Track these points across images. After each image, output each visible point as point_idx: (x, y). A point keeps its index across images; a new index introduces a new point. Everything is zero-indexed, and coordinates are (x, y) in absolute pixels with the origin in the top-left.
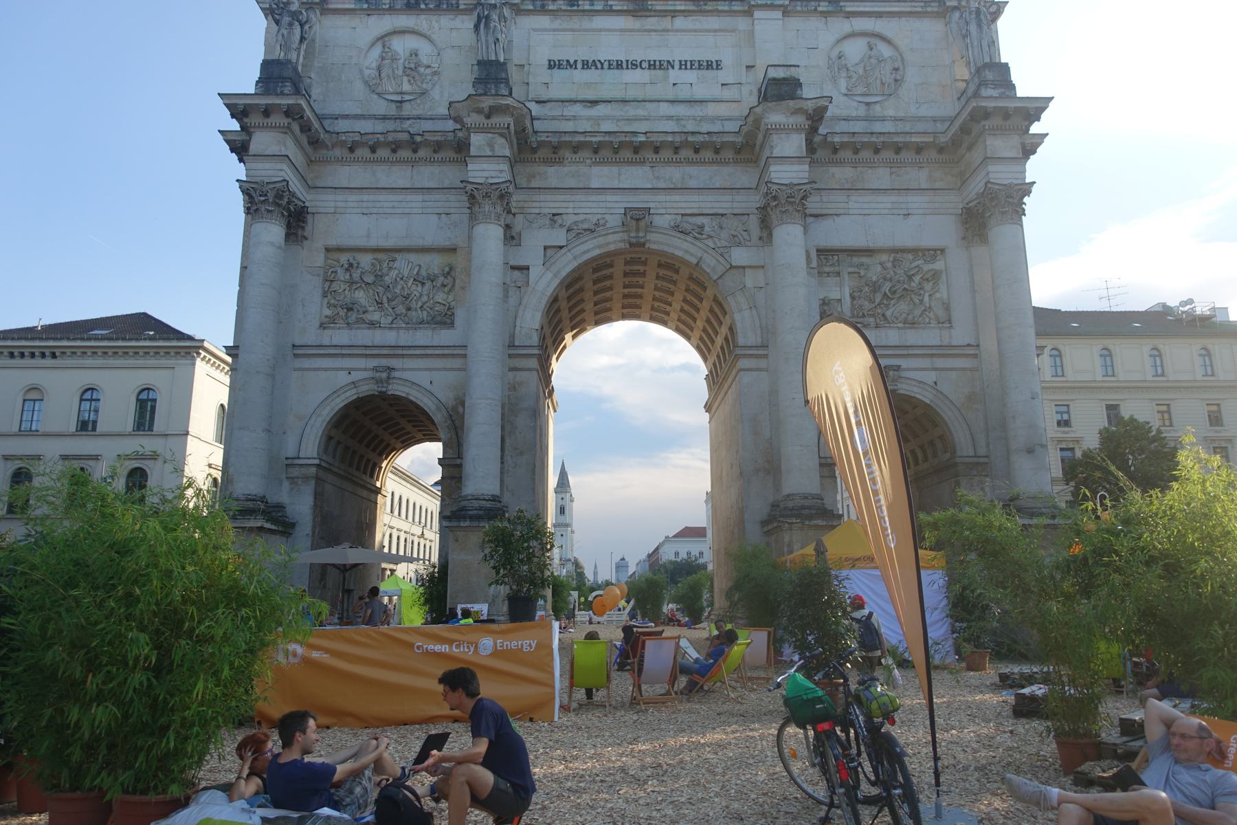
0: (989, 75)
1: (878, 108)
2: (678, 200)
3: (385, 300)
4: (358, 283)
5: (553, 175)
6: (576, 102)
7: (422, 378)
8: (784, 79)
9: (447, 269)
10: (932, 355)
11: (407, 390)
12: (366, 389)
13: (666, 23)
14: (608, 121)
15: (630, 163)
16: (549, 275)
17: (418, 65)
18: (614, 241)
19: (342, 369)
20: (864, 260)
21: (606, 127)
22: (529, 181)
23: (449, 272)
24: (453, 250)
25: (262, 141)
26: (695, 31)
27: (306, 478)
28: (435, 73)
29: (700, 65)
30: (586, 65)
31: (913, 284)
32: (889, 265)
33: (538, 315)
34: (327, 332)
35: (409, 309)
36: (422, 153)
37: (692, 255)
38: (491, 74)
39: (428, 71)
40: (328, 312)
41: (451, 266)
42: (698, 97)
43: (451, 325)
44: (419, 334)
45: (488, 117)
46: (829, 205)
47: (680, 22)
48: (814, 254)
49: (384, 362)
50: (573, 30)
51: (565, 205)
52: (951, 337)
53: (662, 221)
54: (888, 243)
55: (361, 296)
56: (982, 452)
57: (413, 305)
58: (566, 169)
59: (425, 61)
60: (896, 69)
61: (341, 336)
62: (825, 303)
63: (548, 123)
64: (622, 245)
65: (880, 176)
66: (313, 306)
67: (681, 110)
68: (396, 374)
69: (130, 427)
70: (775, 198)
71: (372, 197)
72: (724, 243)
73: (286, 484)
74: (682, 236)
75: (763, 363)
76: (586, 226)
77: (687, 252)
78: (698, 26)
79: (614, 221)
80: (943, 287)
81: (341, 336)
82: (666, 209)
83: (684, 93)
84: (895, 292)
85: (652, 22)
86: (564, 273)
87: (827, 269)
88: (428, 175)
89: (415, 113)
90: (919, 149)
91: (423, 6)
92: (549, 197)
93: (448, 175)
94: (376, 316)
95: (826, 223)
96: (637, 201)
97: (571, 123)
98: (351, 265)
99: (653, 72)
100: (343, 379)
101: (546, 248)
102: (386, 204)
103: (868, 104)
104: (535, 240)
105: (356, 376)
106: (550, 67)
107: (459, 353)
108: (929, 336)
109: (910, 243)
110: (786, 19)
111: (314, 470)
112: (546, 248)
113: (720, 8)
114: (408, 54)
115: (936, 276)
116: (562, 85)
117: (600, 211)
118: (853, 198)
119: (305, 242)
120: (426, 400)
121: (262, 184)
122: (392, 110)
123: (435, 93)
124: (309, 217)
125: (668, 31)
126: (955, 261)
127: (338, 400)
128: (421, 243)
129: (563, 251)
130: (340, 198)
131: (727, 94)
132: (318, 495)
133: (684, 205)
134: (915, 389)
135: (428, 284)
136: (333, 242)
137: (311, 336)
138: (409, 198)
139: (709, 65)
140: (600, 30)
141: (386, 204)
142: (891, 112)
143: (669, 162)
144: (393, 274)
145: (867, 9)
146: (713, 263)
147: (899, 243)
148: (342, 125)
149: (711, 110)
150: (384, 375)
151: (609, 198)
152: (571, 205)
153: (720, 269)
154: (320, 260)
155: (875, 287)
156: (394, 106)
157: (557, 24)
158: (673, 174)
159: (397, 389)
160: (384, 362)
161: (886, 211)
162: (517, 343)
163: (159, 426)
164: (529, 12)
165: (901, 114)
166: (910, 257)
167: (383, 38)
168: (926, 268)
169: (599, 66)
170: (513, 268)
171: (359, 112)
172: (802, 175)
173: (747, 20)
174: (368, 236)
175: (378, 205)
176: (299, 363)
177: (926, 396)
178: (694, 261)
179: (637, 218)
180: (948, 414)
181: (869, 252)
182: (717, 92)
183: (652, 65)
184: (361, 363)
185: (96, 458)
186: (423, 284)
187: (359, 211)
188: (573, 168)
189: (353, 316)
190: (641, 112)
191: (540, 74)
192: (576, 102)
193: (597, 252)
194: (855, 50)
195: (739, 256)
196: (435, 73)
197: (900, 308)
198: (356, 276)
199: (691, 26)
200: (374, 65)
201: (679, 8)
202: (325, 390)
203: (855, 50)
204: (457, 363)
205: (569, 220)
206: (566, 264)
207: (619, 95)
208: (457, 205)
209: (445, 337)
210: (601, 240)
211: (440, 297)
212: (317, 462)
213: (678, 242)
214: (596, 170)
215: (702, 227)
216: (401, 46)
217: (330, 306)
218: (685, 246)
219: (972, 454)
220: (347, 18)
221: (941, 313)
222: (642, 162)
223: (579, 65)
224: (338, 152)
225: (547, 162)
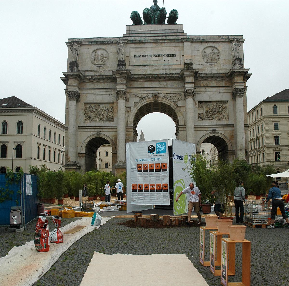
0: (237, 62)
1: (213, 66)
2: (166, 92)
3: (98, 115)
4: (91, 111)
5: (136, 84)
6: (141, 66)
7: (107, 134)
8: (189, 63)
9: (112, 107)
10: (223, 127)
11: (104, 136)
12: (95, 136)
13: (163, 45)
14: (148, 71)
15: (154, 81)
16: (135, 109)
17: (103, 57)
18: (150, 100)
19: (89, 132)
20: (209, 104)
21: (149, 72)
22: (130, 86)
23: (112, 108)
24: (113, 103)
25: (71, 82)
26: (170, 47)
27: (83, 156)
28: (107, 59)
29: (171, 56)
30: (143, 56)
31: (220, 110)
32: (215, 105)
33: (133, 119)
34: (86, 123)
35: (103, 117)
36: (105, 80)
37: (168, 103)
38: (121, 63)
39: (106, 58)
40: (85, 118)
41: (112, 106)
42: (170, 64)
43: (113, 121)
44: (106, 123)
45: (121, 75)
46: (201, 91)
47: (166, 45)
49: (99, 130)
50: (140, 47)
51: (139, 92)
52: (228, 122)
53: (161, 95)
54: (215, 100)
55: (92, 114)
56: (234, 149)
57: (104, 116)
58: (139, 83)
59: (105, 56)
60: (218, 56)
61: (89, 124)
62: (200, 114)
63: (134, 72)
64: (152, 101)
65: (213, 83)
66: (83, 118)
67: (166, 67)
68: (101, 133)
69: (16, 133)
70: (187, 92)
71: (94, 91)
72: (176, 101)
73: (79, 158)
74: (166, 99)
75: (184, 129)
76: (144, 97)
77: (167, 102)
78: (170, 46)
79: (150, 95)
80: (227, 110)
81: (89, 124)
82: (162, 93)
84: (216, 112)
85: (159, 45)
86: (139, 108)
87: (200, 106)
88: (107, 85)
90: (222, 77)
91: (104, 43)
92: (135, 90)
93: (111, 85)
95: (200, 95)
96: (156, 91)
97: (140, 71)
98: (90, 107)
99: (159, 57)
100: (90, 134)
101: (134, 102)
102: (97, 92)
103: (211, 65)
104: (132, 100)
106: (135, 57)
107: (115, 127)
108: (223, 122)
109: (220, 100)
110: (192, 43)
111: (84, 154)
112: (134, 102)
113: (175, 41)
114: (101, 54)
115: (226, 108)
116: (138, 61)
117: (147, 93)
118: (207, 89)
119: (80, 102)
120: (108, 138)
121: (72, 92)
123: (108, 64)
124: (80, 96)
125: (163, 47)
126: (230, 105)
127: (89, 139)
128: (106, 102)
129: (138, 103)
130: (86, 91)
131: (177, 63)
132: (85, 160)
133: (166, 91)
134: (219, 135)
135: (108, 111)
136: (86, 102)
137: (82, 124)
138: (103, 91)
139: (173, 56)
140: (147, 47)
141: (97, 92)
143: (163, 81)
144: (99, 109)
145: (211, 41)
146: (173, 105)
147: (217, 100)
148: (87, 74)
149: (174, 67)
150: (99, 133)
151: (149, 90)
152: (140, 92)
153: (175, 107)
154: (83, 106)
155: (212, 110)
156: (98, 68)
157: (136, 46)
158: (164, 83)
159: (102, 136)
160: (99, 130)
161: (215, 92)
162: (128, 125)
163: (24, 132)
164: (130, 43)
166: (220, 103)
167: (95, 51)
168: (223, 105)
169: (146, 56)
170: (127, 107)
171: (90, 70)
172: (192, 87)
173: (182, 44)
174: (94, 100)
175: (95, 93)
176: (80, 131)
177: (222, 136)
178: (169, 105)
179: (155, 95)
180: (226, 141)
181: (210, 102)
182: (175, 62)
183: (159, 56)
184: (93, 130)
185: (8, 142)
186: (106, 111)
187: (91, 94)
188: (141, 82)
189: (91, 119)
190: (156, 68)
191: (133, 59)
192: (141, 66)
193: (146, 103)
194: (209, 51)
195: (179, 104)
196: (107, 59)
198: (91, 110)
199: (169, 46)
200: (93, 57)
201: (165, 41)
202: (86, 137)
204: (115, 130)
205: (139, 95)
206: (139, 106)
207: (151, 64)
208: (114, 92)
209: (112, 124)
210: (147, 100)
211: (110, 114)
212: (85, 153)
213: (165, 100)
214: (146, 83)
215: (171, 96)
216: (99, 52)
217: (86, 117)
218: (167, 101)
219: (231, 150)
220: (86, 46)
221: (226, 116)
222: (157, 81)
223: (142, 56)
224: (86, 80)
225: (135, 81)
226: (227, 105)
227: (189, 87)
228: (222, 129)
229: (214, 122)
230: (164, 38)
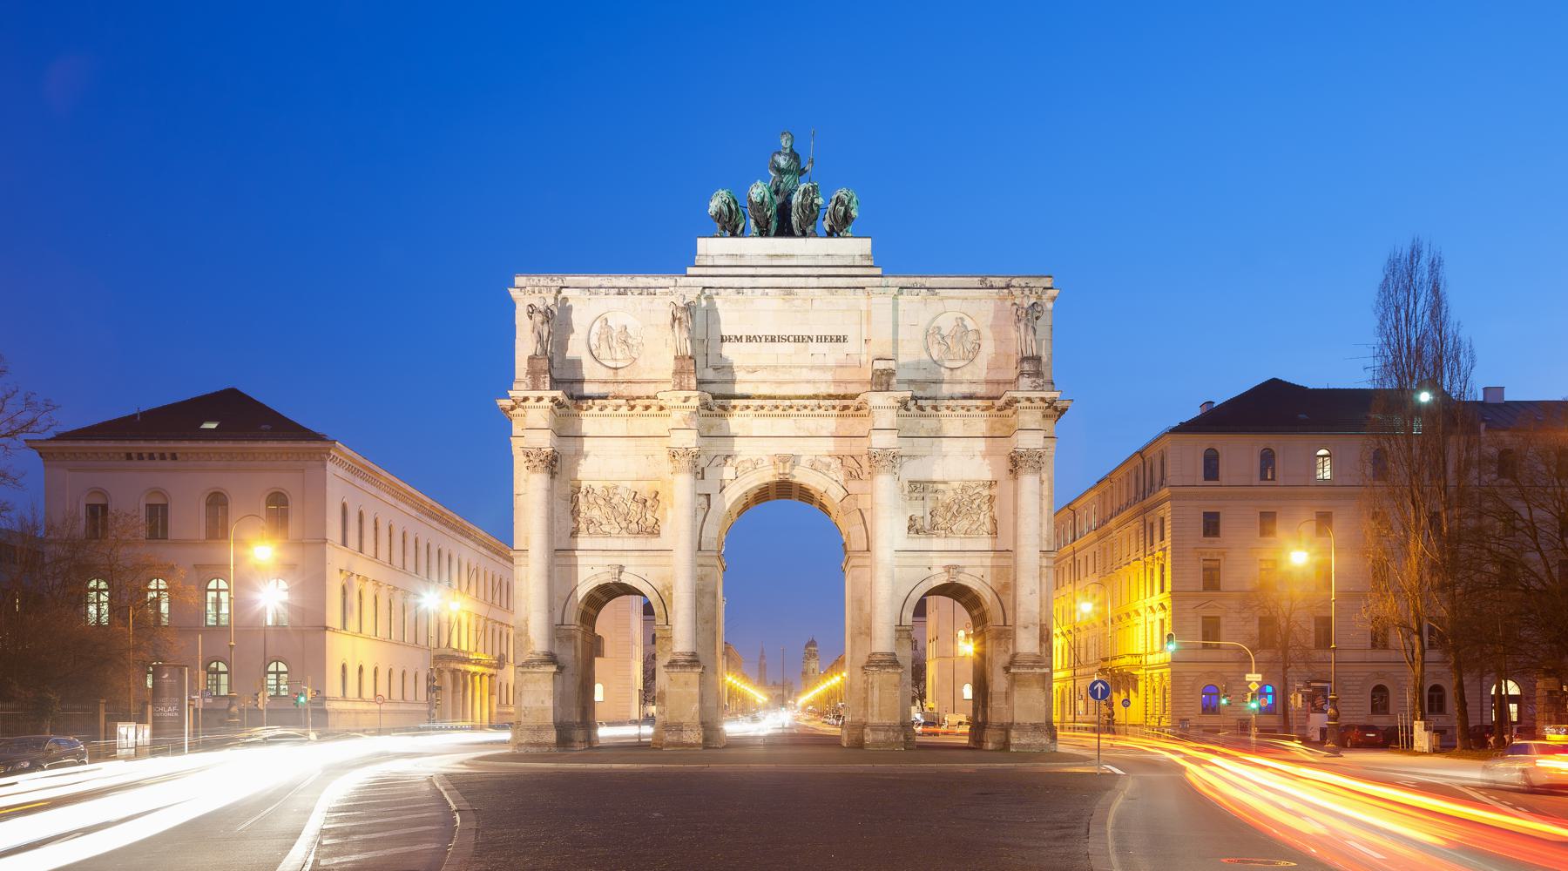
12: (606, 578)
20: (941, 487)
30: (749, 339)
48: (906, 485)
53: (804, 461)
67: (816, 375)
83: (819, 361)
89: (628, 377)
94: (606, 528)
96: (787, 448)
105: (597, 570)
122: (609, 375)
123: (640, 362)
139: (838, 340)
142: (968, 377)
158: (810, 424)
165: (975, 378)
181: (945, 482)
183: (797, 339)
184: (600, 561)
190: (788, 377)
197: (963, 524)
203: (947, 324)
215: (829, 465)
221: (988, 526)
226: (994, 491)
227: (881, 441)
228: (977, 561)
229: (955, 544)
230: (813, 282)
